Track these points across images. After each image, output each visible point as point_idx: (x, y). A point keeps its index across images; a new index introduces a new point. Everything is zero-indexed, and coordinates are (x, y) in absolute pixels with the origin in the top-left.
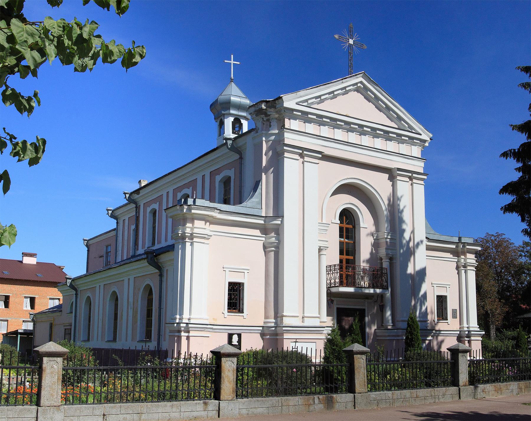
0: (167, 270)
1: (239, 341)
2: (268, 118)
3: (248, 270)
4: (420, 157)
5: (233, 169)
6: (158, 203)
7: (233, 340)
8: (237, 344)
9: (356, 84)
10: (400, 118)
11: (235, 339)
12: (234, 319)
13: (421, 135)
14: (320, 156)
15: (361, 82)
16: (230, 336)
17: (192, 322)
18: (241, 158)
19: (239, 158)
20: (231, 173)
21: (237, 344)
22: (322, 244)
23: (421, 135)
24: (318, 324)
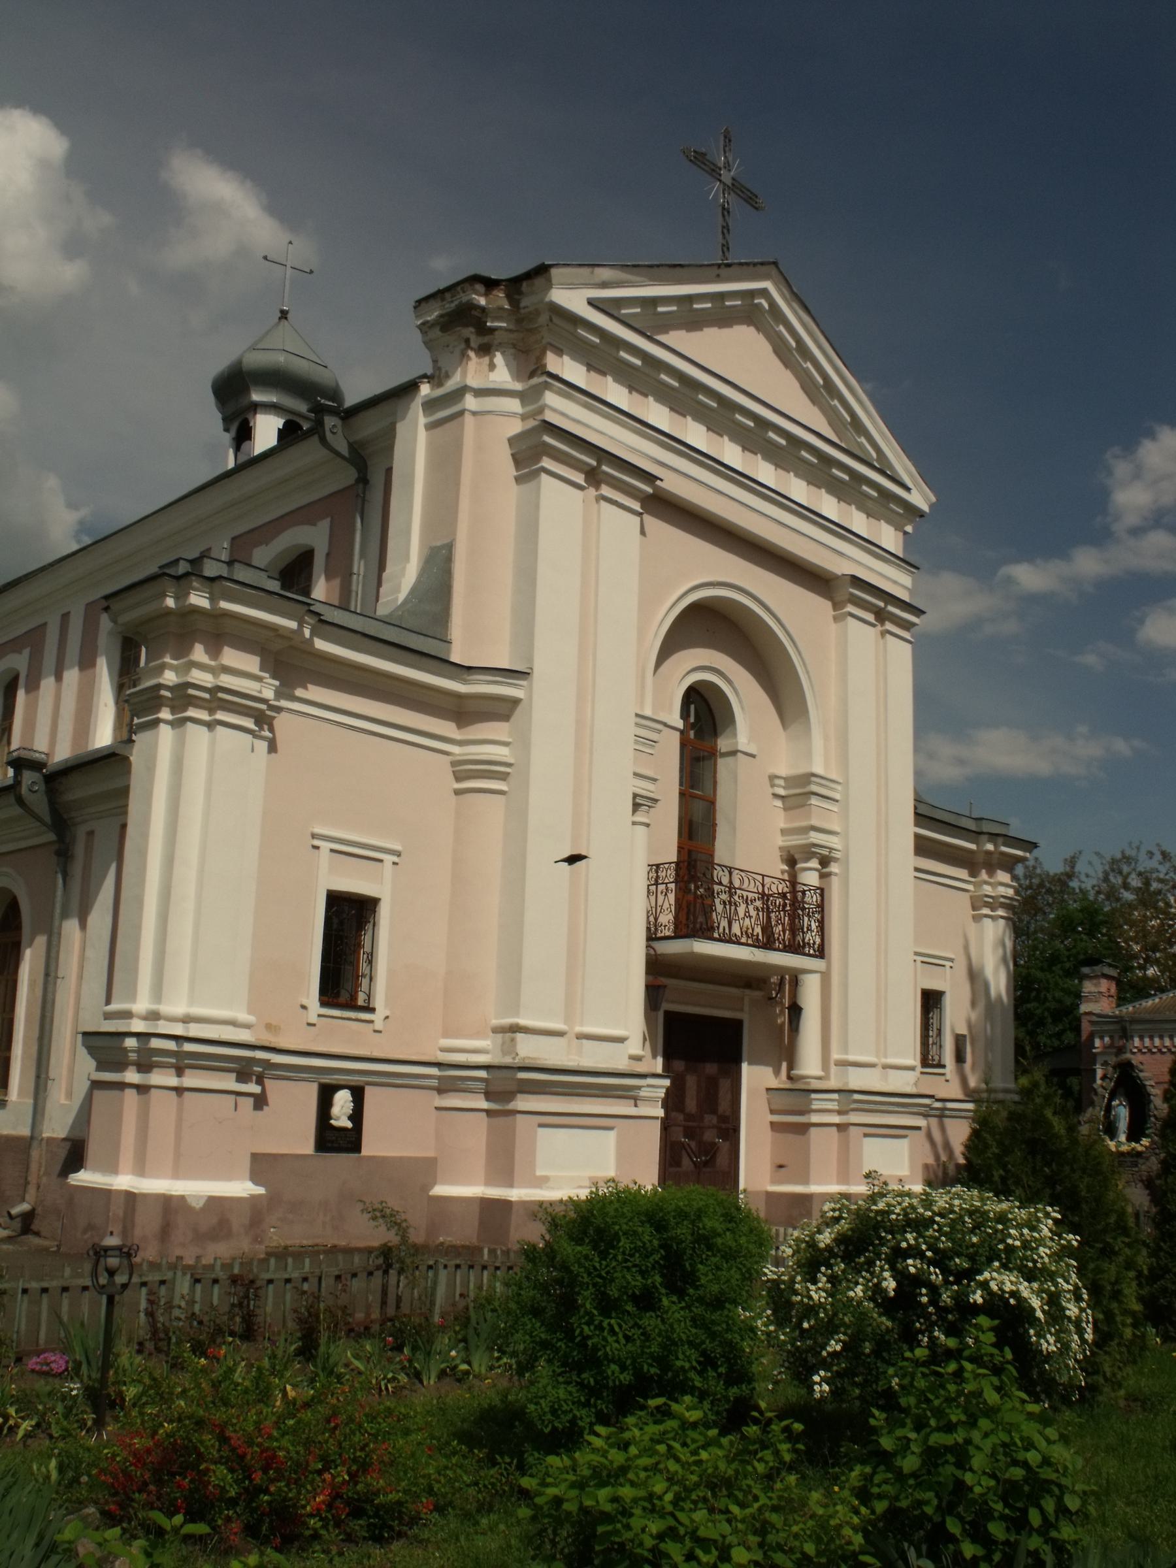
0: (91, 833)
1: (357, 1116)
2: (486, 339)
3: (398, 854)
4: (901, 556)
5: (324, 525)
6: (26, 652)
7: (336, 1110)
8: (349, 1125)
9: (752, 294)
10: (857, 425)
11: (342, 1101)
12: (341, 1035)
13: (908, 489)
14: (650, 490)
15: (764, 293)
16: (326, 1094)
17: (194, 1030)
18: (363, 480)
19: (358, 481)
20: (316, 536)
21: (349, 1125)
22: (644, 787)
23: (908, 489)
24: (622, 1065)
